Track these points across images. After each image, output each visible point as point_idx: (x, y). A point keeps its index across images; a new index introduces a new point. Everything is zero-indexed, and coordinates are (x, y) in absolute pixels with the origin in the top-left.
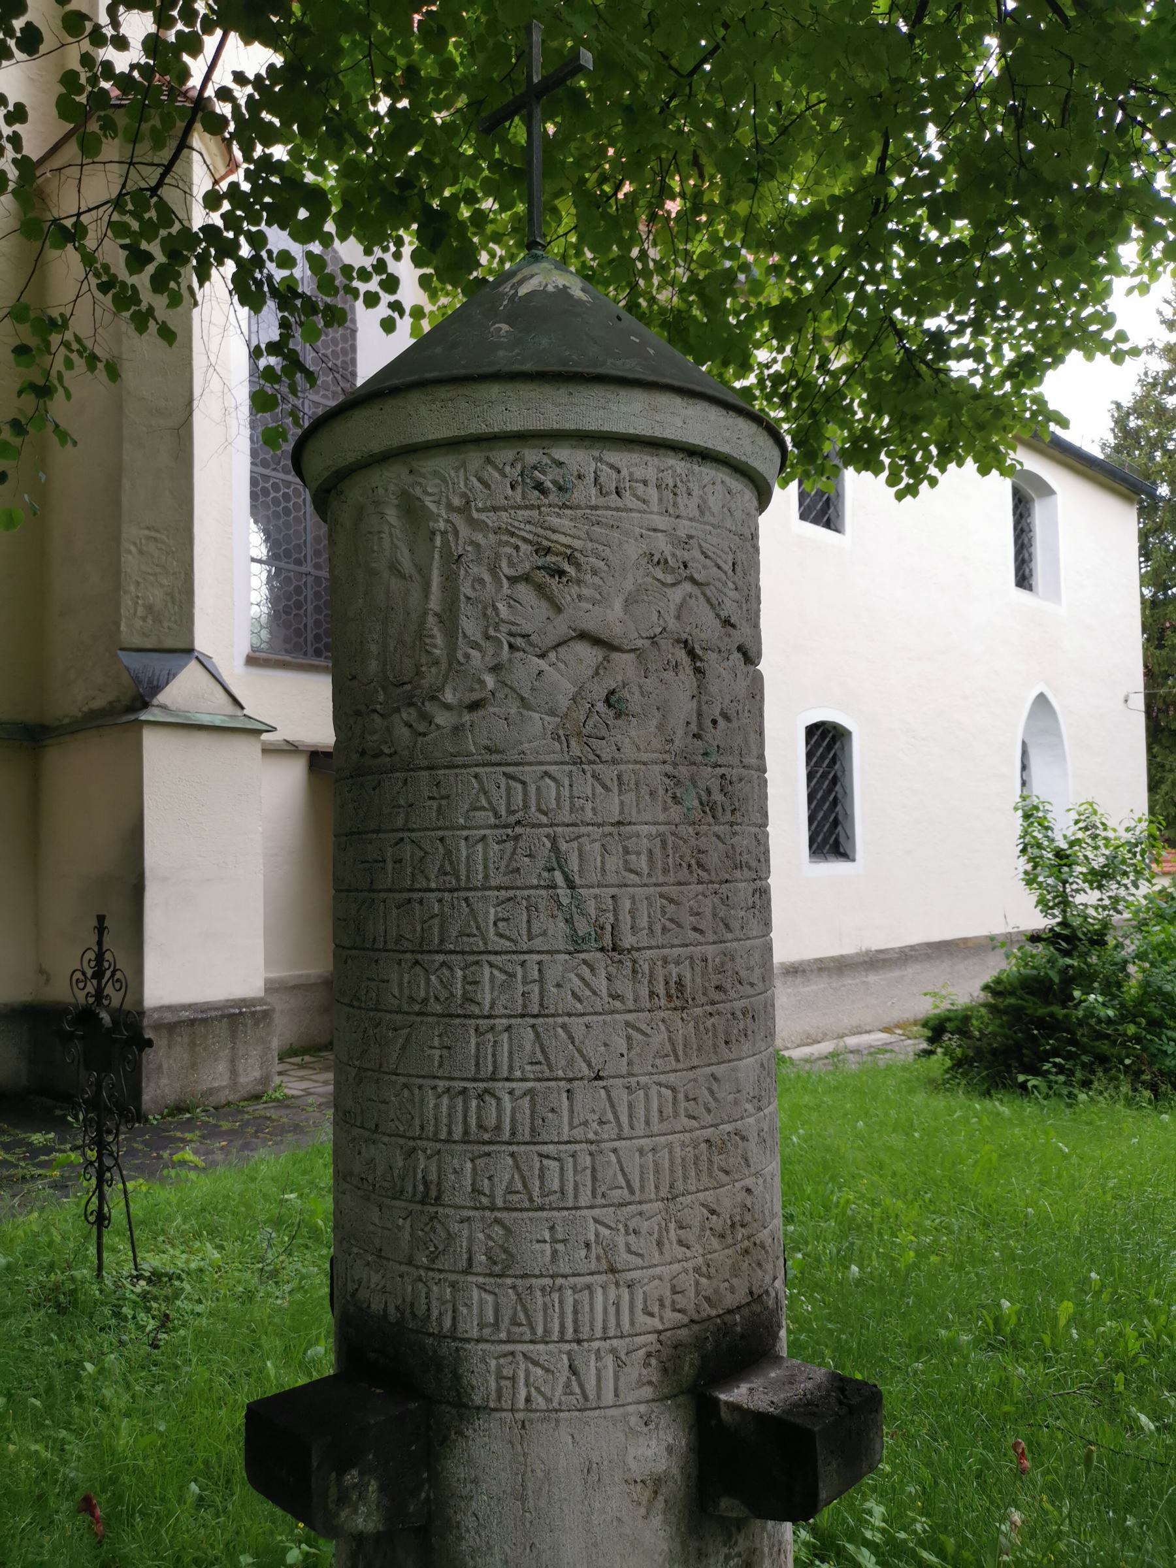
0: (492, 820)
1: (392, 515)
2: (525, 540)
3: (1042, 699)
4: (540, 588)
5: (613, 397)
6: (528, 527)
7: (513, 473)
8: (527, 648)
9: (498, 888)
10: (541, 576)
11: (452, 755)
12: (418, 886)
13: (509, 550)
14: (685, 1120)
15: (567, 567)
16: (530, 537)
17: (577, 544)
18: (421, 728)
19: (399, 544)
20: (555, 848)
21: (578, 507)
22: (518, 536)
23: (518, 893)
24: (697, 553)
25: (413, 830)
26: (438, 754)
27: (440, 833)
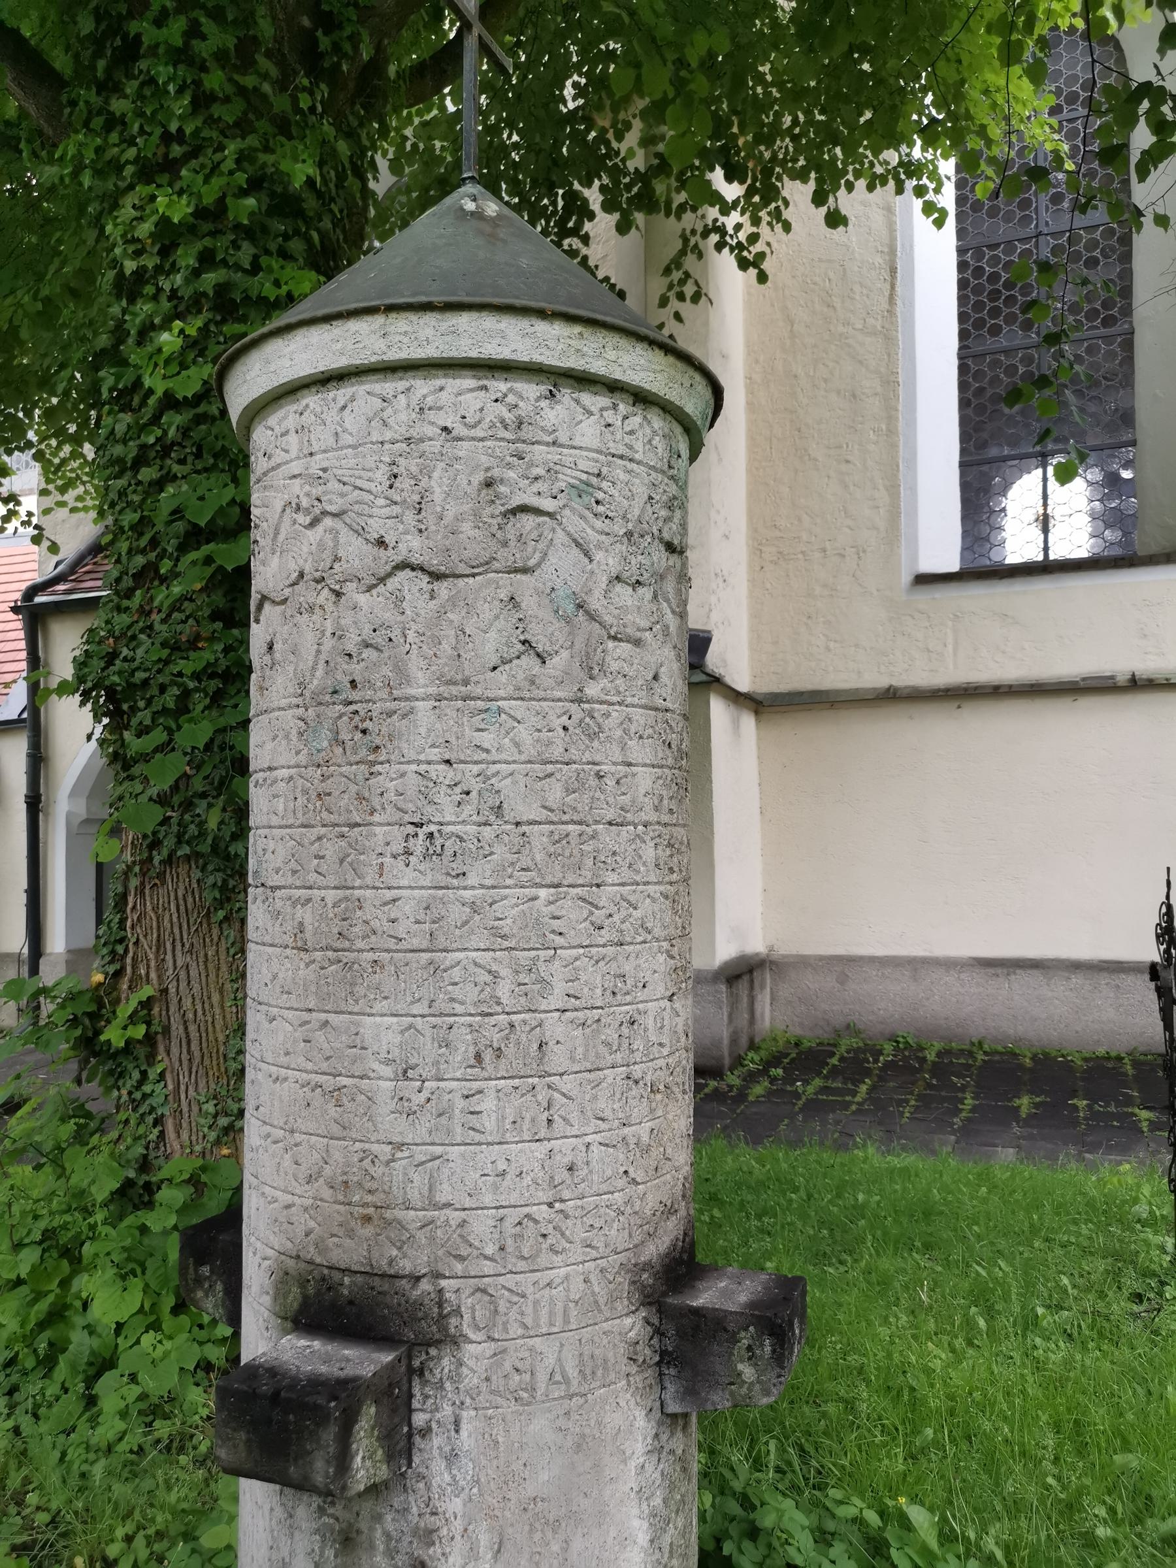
5: (244, 369)
14: (301, 1060)
24: (334, 485)
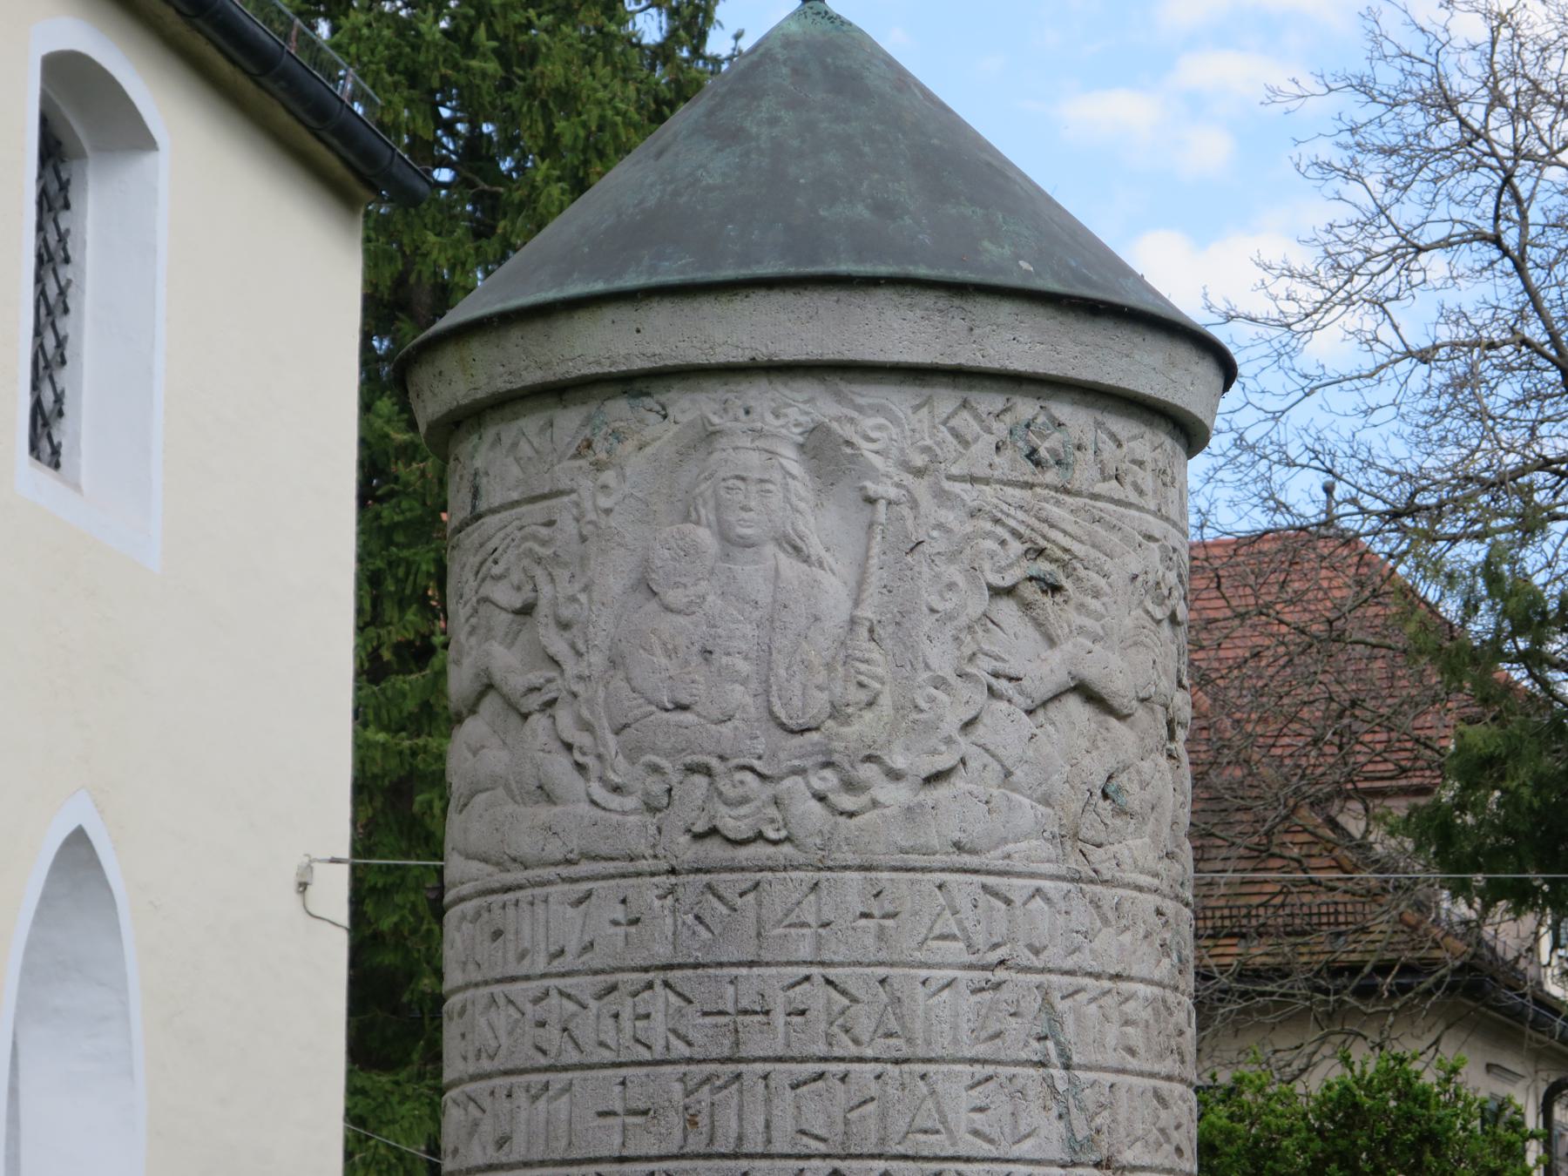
0: (968, 958)
1: (791, 460)
2: (1017, 535)
3: (78, 840)
4: (1027, 606)
6: (1020, 515)
7: (1000, 429)
8: (1017, 698)
9: (973, 1061)
10: (1030, 592)
11: (903, 851)
12: (837, 1052)
13: (991, 545)
15: (1067, 584)
16: (1022, 529)
17: (1076, 547)
18: (847, 802)
19: (802, 506)
20: (1047, 1005)
21: (1078, 494)
22: (1004, 525)
23: (1000, 1069)
25: (831, 964)
26: (879, 848)
27: (882, 971)
